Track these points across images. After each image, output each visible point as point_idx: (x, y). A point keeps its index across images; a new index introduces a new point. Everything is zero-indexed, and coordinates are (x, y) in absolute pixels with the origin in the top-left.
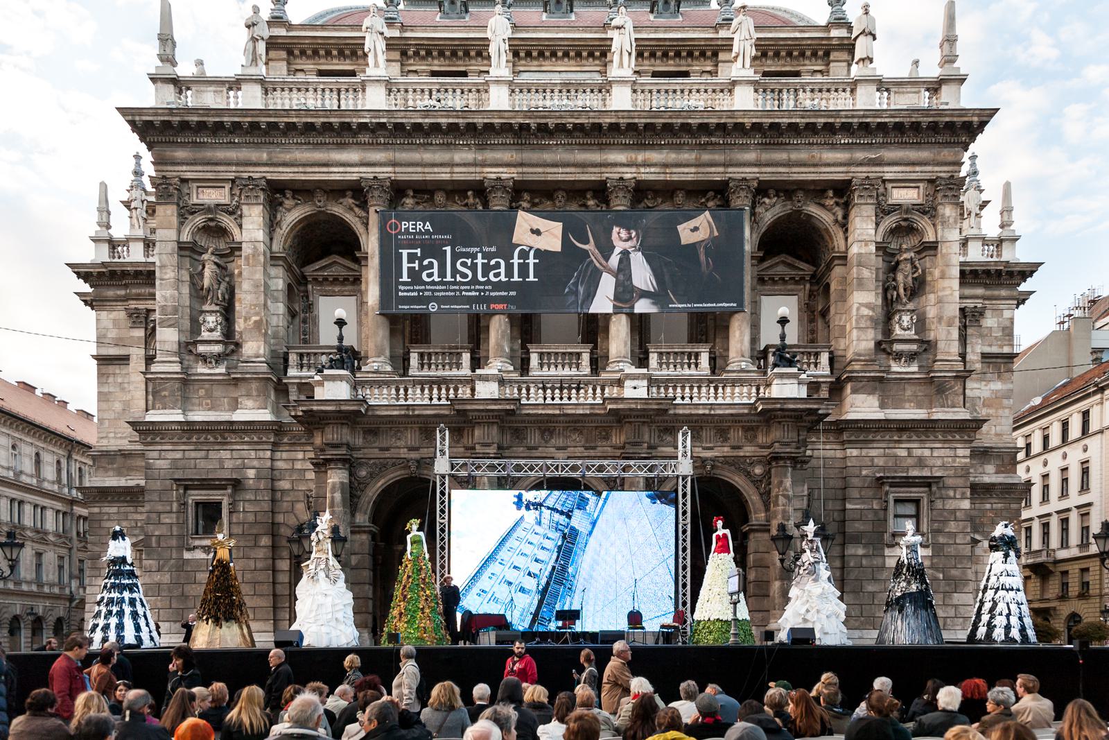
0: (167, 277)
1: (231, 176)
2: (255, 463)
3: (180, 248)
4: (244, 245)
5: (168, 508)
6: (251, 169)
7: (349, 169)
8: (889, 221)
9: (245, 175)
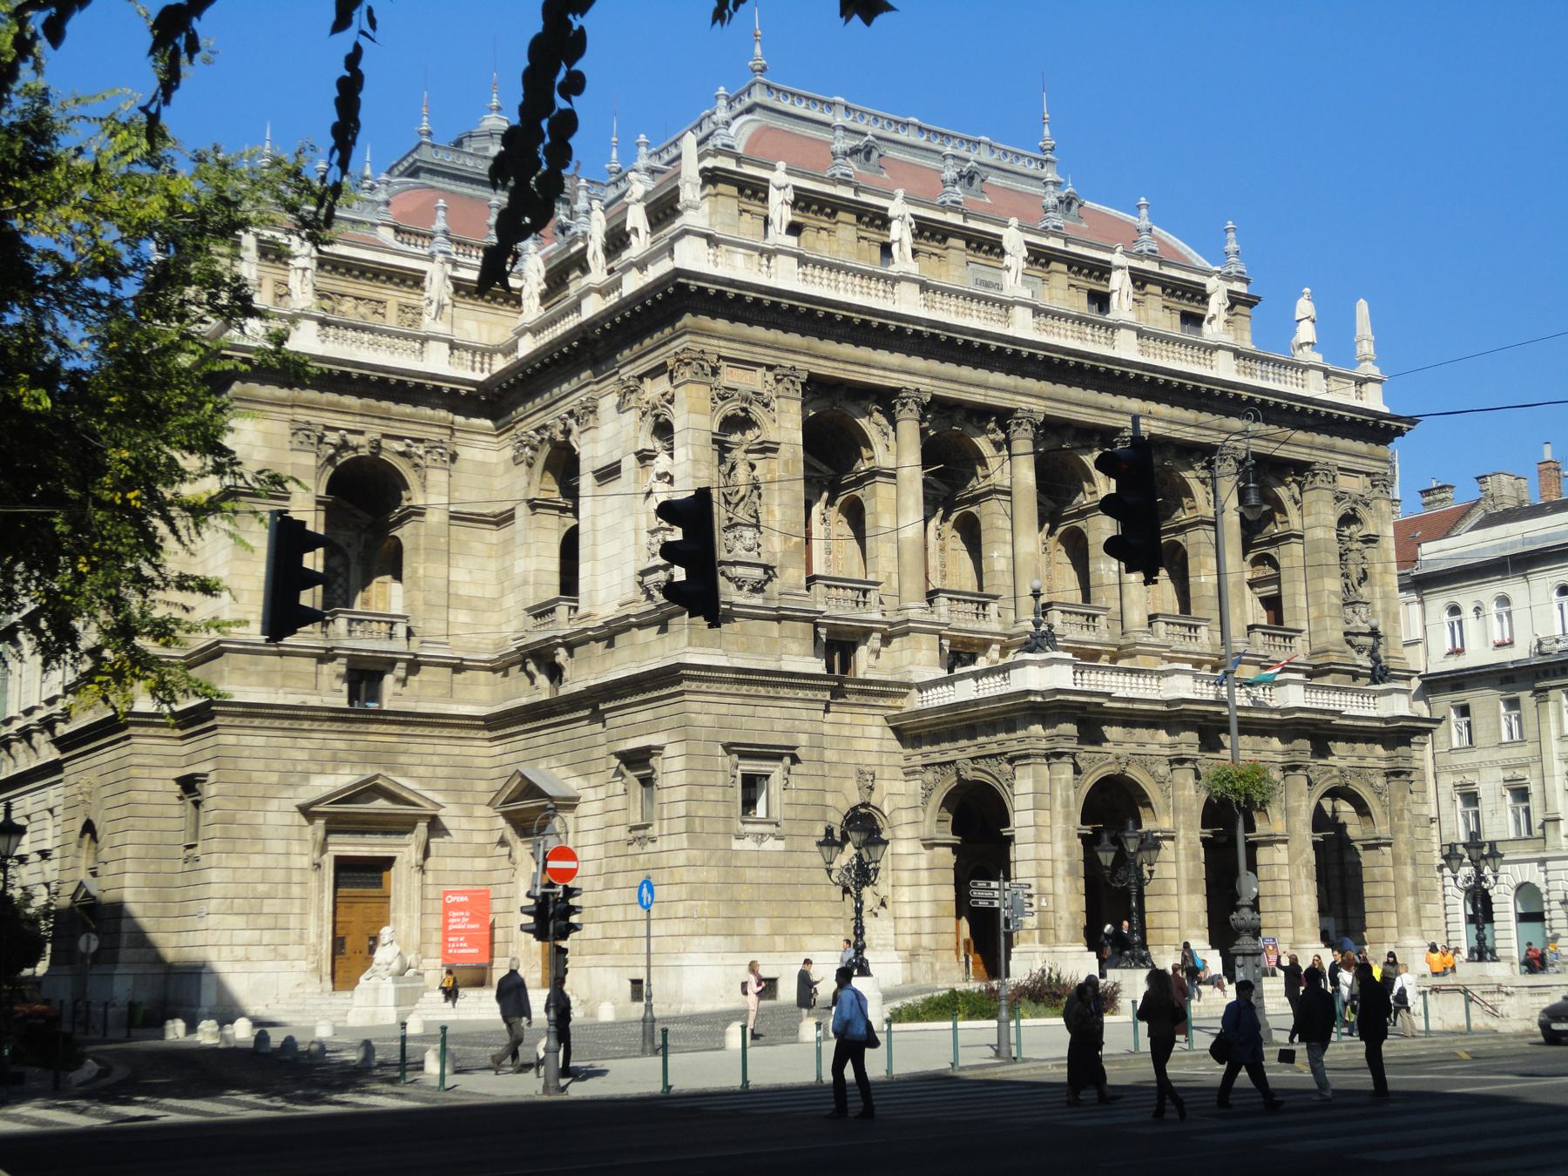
0: (700, 474)
1: (769, 361)
2: (807, 726)
3: (714, 441)
4: (782, 447)
5: (712, 781)
6: (791, 356)
7: (888, 374)
8: (1343, 508)
9: (789, 364)
